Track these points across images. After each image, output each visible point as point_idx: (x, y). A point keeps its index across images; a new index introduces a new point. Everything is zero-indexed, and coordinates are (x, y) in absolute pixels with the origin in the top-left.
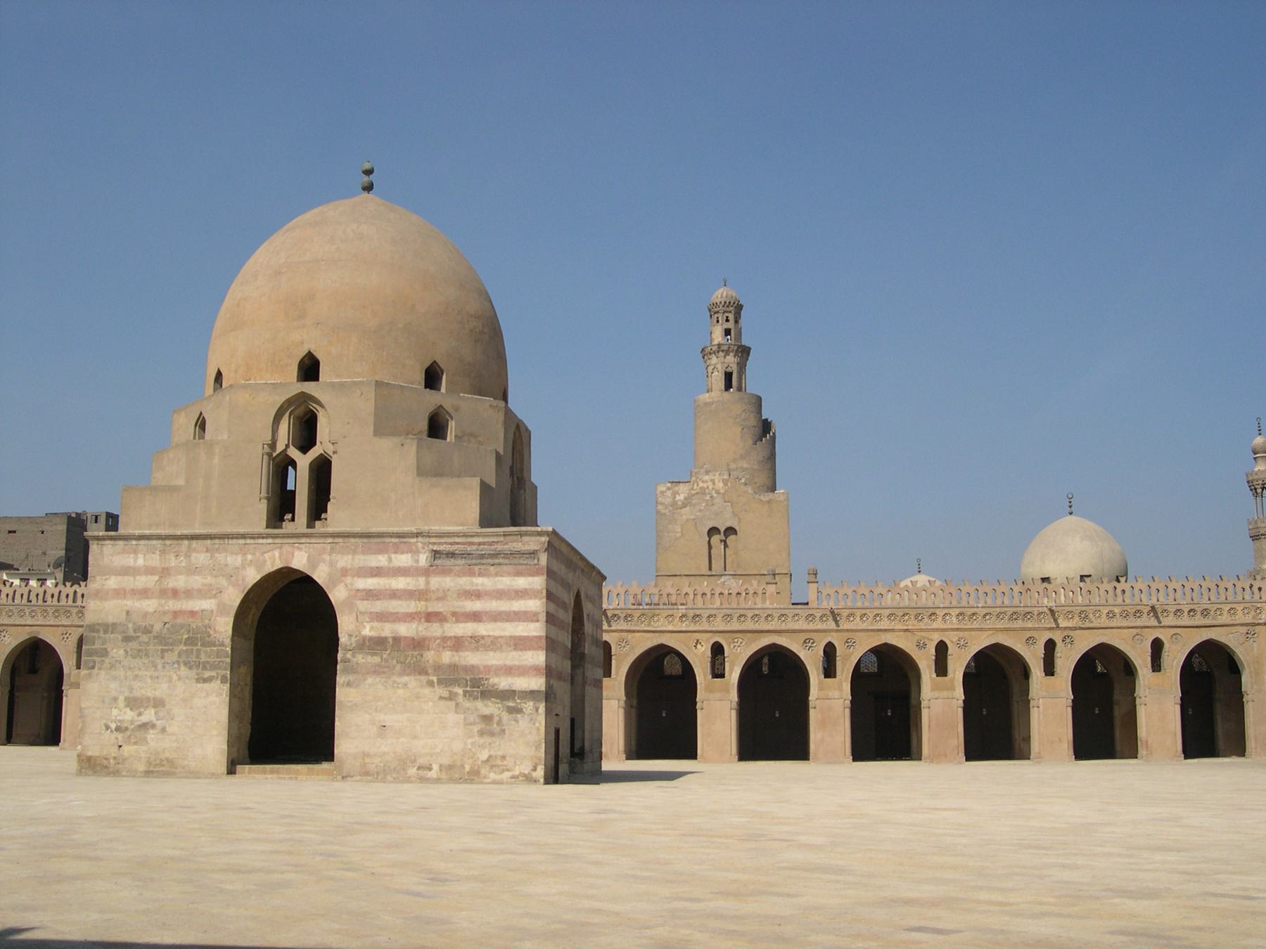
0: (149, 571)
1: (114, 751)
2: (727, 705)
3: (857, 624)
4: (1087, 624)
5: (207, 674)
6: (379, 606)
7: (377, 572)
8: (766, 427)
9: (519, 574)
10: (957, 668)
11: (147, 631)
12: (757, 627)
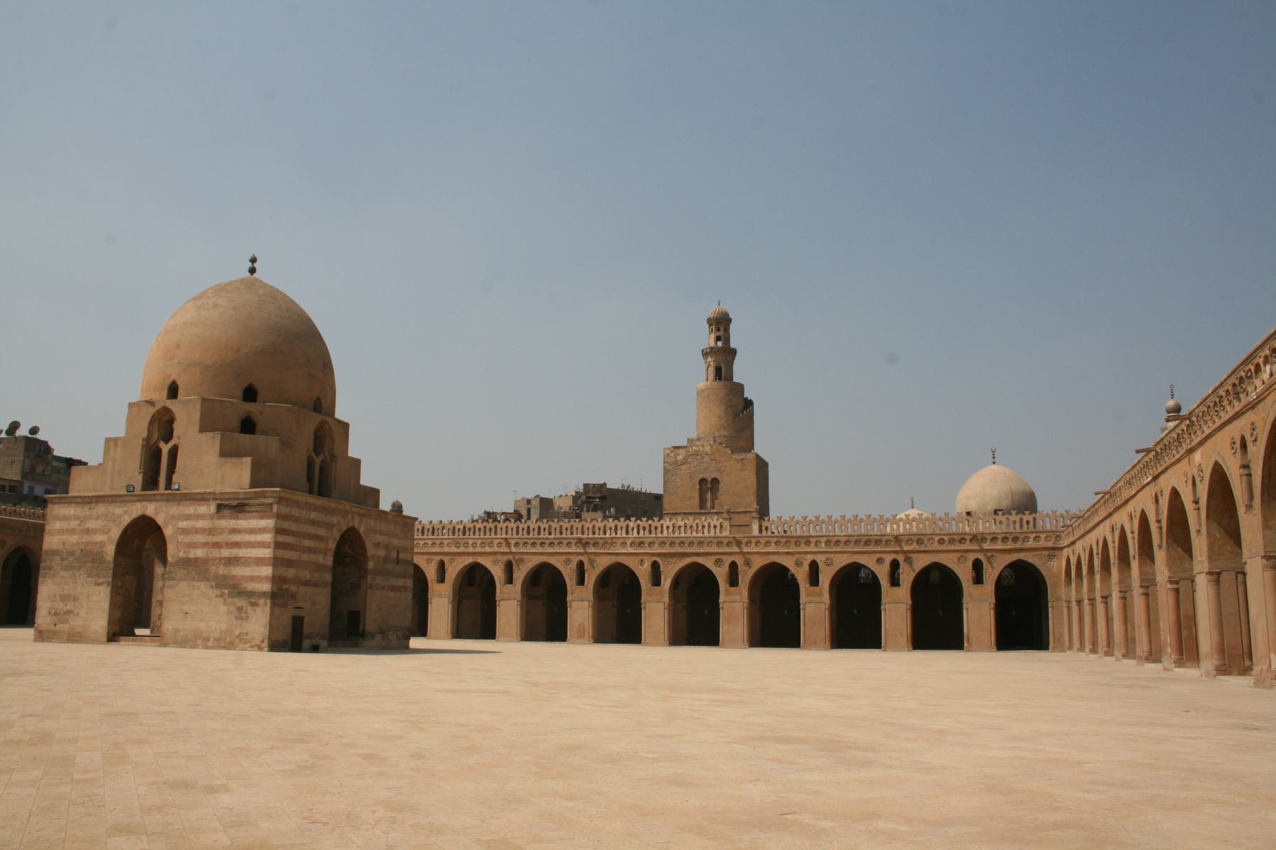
0: (77, 518)
1: (52, 627)
2: (661, 606)
3: (753, 549)
4: (922, 548)
5: (102, 580)
6: (188, 539)
7: (188, 517)
8: (749, 404)
9: (261, 518)
10: (825, 579)
11: (72, 554)
12: (682, 550)
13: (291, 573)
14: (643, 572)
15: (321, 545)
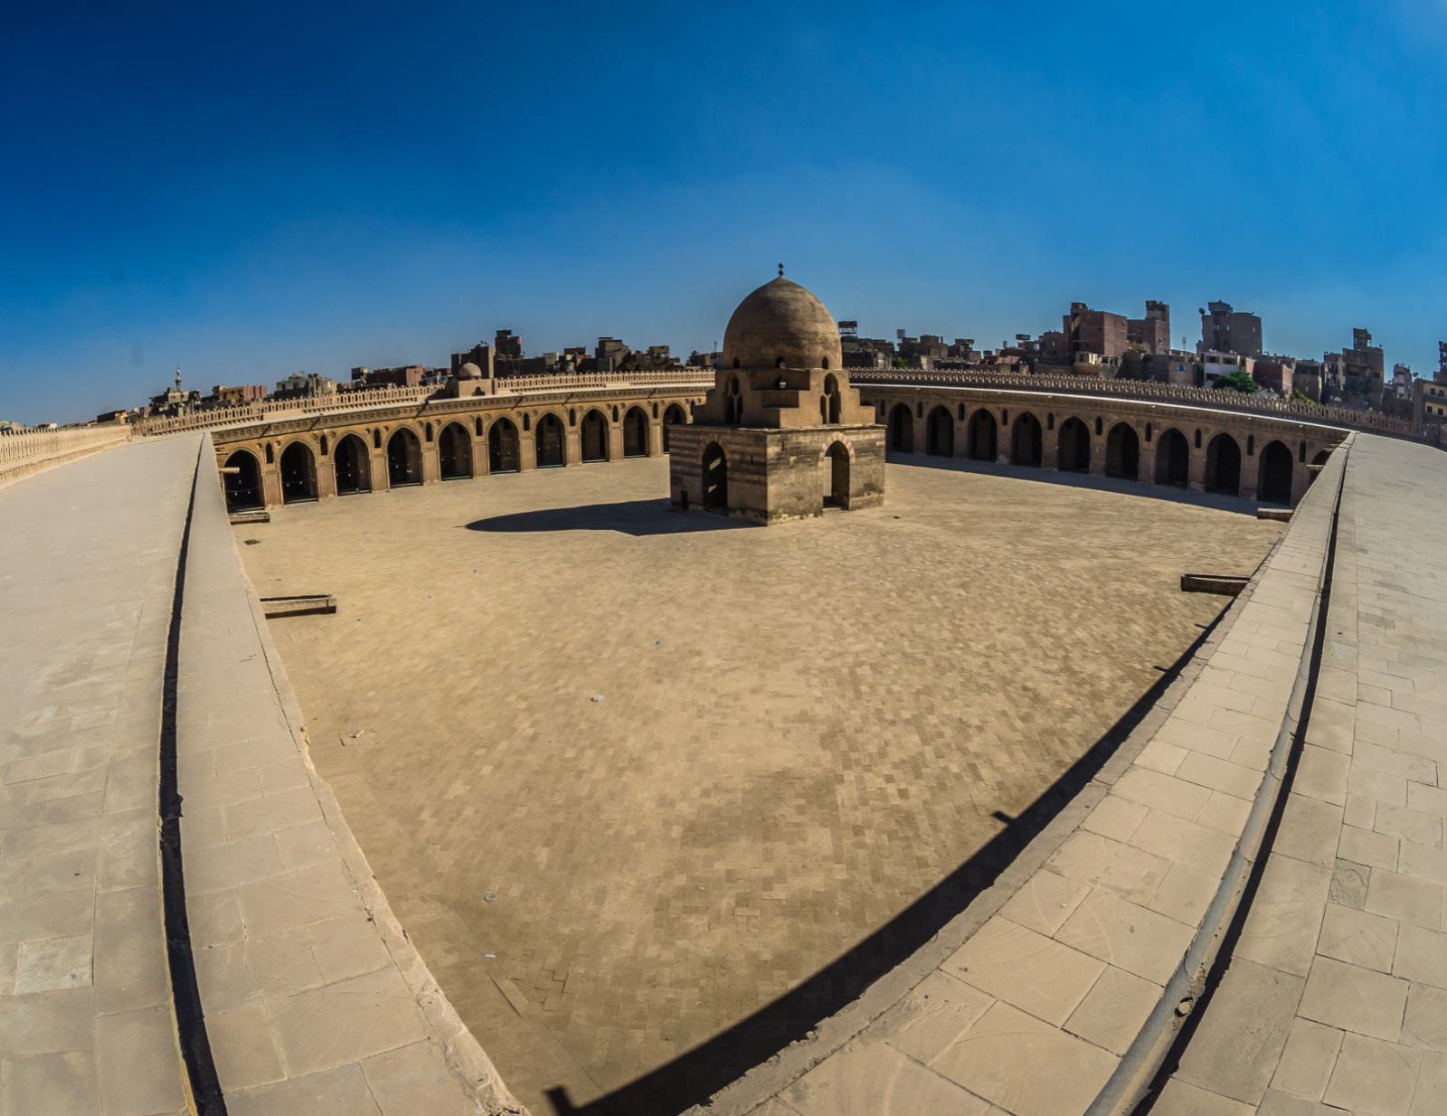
13: (679, 468)
15: (692, 453)
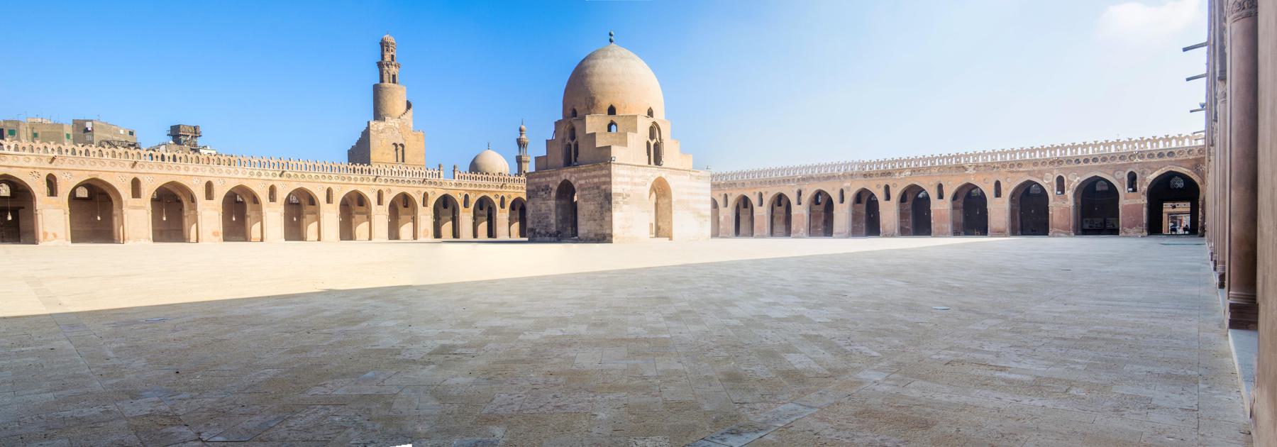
14: (460, 200)
